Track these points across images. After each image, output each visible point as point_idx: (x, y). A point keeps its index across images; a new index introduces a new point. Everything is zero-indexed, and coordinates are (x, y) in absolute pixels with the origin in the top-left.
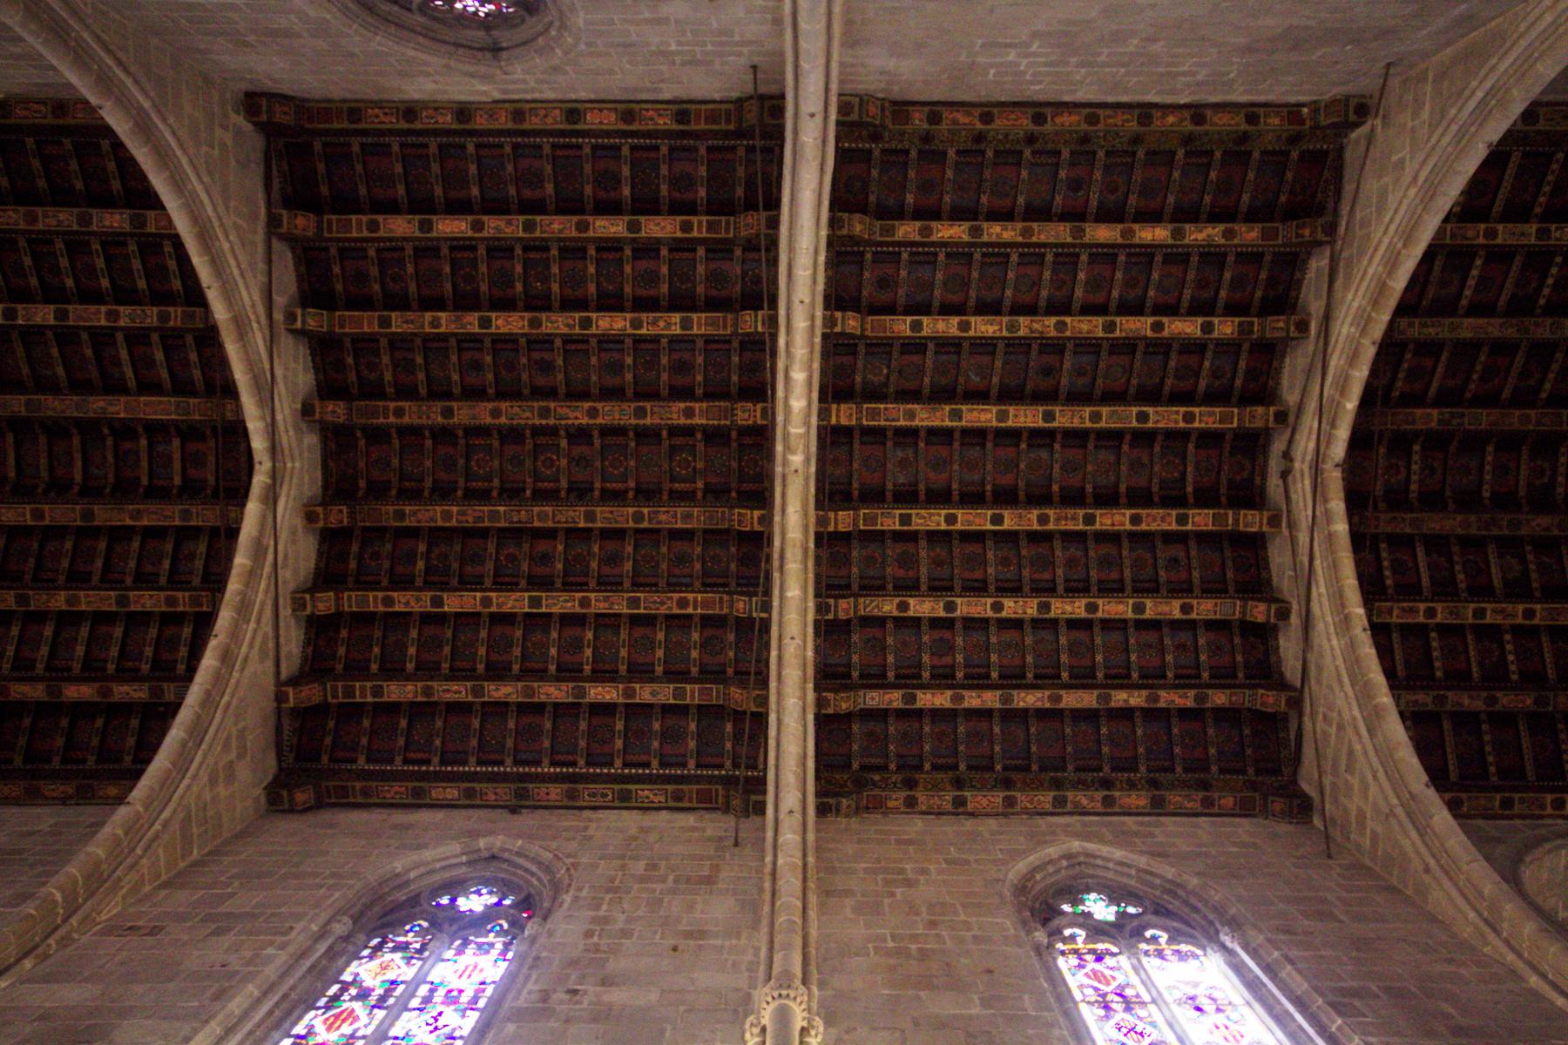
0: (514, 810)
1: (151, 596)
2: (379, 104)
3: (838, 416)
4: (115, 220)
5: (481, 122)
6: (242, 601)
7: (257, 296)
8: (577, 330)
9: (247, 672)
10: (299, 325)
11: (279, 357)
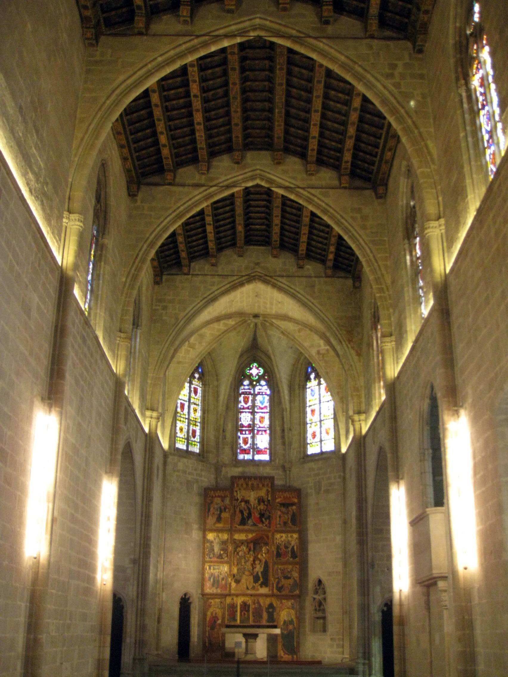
2: (124, 166)
3: (232, 5)
4: (180, 239)
5: (124, 142)
7: (197, 192)
8: (199, 99)
9: (331, 204)
10: (205, 172)
11: (217, 178)
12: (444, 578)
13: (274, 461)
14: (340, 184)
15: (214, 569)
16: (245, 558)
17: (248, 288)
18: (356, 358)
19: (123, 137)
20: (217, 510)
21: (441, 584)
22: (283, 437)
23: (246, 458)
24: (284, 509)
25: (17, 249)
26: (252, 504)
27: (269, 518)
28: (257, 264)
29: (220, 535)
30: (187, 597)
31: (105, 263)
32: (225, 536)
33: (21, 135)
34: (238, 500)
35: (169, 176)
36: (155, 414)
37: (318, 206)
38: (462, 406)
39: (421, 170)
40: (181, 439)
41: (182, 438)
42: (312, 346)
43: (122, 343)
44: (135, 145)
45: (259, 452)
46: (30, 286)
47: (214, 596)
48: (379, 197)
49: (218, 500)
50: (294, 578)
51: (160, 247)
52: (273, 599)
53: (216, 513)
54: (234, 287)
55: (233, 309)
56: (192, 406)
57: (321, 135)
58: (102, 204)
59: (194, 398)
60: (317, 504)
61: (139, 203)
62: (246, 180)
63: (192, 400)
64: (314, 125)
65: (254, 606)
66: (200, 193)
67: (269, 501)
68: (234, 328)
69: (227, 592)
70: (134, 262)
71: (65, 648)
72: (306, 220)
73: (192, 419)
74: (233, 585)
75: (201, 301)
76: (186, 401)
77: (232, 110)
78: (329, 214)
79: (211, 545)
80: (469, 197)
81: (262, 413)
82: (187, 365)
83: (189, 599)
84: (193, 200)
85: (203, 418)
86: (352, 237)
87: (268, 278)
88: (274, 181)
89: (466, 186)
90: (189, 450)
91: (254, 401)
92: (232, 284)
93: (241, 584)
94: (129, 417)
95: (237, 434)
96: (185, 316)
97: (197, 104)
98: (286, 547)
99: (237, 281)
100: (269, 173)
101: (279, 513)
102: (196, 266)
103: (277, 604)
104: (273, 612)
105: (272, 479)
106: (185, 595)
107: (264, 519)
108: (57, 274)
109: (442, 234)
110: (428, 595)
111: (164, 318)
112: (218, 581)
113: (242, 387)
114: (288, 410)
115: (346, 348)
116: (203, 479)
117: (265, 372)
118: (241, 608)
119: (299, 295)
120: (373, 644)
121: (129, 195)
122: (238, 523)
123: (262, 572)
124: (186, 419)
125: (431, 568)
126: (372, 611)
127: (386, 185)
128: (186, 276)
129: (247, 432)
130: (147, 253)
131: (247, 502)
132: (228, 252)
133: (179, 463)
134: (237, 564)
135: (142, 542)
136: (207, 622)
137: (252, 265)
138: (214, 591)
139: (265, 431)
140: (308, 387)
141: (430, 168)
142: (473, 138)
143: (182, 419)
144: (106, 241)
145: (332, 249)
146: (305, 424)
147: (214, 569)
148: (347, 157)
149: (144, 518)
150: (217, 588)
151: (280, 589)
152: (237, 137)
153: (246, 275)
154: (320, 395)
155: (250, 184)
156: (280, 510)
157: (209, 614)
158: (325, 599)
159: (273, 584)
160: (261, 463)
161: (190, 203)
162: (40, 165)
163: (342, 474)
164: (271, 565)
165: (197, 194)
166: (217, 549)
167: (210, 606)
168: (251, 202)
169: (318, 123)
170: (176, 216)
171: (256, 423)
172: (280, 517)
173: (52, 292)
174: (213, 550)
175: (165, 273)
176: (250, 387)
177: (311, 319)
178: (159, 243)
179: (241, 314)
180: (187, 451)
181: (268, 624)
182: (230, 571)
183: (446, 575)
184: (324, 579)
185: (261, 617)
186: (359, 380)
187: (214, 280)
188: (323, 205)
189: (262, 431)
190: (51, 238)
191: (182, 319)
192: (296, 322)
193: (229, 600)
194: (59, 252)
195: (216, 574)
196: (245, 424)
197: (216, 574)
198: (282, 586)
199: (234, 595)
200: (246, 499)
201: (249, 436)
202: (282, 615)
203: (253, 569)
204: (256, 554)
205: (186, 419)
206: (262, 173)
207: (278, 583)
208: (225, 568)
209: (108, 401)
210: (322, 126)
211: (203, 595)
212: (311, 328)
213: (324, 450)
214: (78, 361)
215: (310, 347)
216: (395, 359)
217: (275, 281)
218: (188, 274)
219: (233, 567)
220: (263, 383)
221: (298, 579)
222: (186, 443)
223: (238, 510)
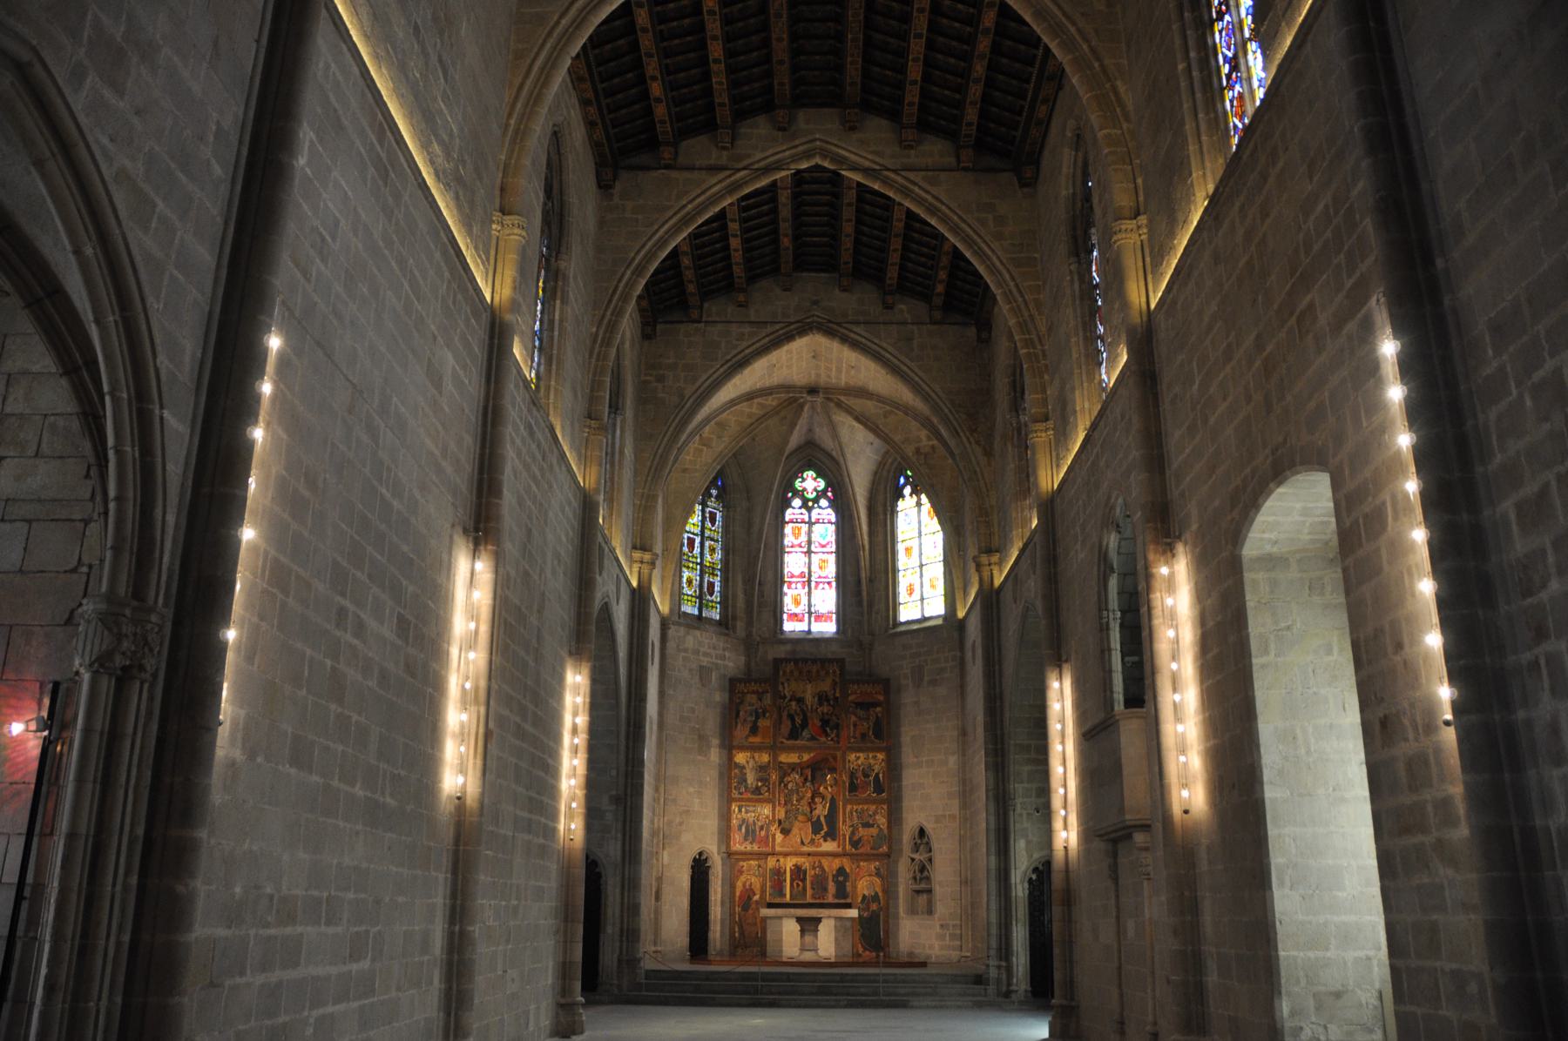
0: (1060, 87)
2: (590, 137)
5: (590, 95)
6: (902, 192)
7: (714, 180)
8: (718, 17)
11: (749, 156)
12: (1146, 827)
14: (959, 161)
15: (747, 812)
16: (798, 793)
17: (801, 345)
19: (588, 85)
20: (751, 715)
21: (1139, 838)
22: (859, 593)
24: (861, 713)
25: (417, 273)
26: (809, 704)
27: (837, 726)
28: (815, 303)
29: (756, 755)
30: (704, 857)
31: (562, 302)
32: (765, 758)
33: (418, 75)
34: (785, 697)
35: (666, 153)
36: (647, 557)
37: (920, 201)
38: (1179, 537)
39: (1105, 131)
41: (692, 596)
43: (592, 437)
44: (609, 100)
45: (819, 618)
46: (439, 338)
48: (1023, 185)
50: (878, 826)
51: (652, 276)
52: (845, 860)
53: (749, 719)
54: (776, 343)
55: (776, 379)
56: (707, 544)
57: (926, 78)
58: (555, 202)
61: (616, 200)
62: (797, 158)
63: (707, 533)
64: (915, 60)
65: (813, 872)
66: (720, 181)
67: (836, 699)
68: (775, 411)
69: (769, 850)
70: (610, 301)
71: (510, 946)
72: (898, 225)
74: (779, 837)
76: (696, 535)
77: (774, 36)
79: (741, 772)
80: (1194, 175)
84: (708, 194)
85: (725, 561)
86: (980, 254)
87: (835, 327)
88: (845, 158)
89: (1188, 156)
91: (809, 533)
92: (772, 337)
93: (791, 835)
94: (606, 562)
96: (693, 394)
97: (714, 26)
98: (866, 776)
99: (781, 332)
100: (836, 145)
101: (853, 718)
104: (846, 880)
105: (841, 662)
106: (700, 854)
108: (485, 317)
109: (1142, 241)
110: (1115, 855)
111: (660, 395)
112: (754, 831)
113: (789, 511)
114: (867, 547)
115: (968, 445)
116: (726, 662)
119: (887, 355)
120: (1015, 934)
121: (600, 186)
122: (786, 735)
123: (825, 817)
124: (697, 564)
125: (1122, 810)
126: (1013, 881)
127: (1037, 163)
128: (696, 325)
129: (799, 586)
130: (631, 285)
131: (800, 701)
134: (785, 804)
136: (737, 899)
138: (749, 847)
139: (829, 583)
140: (899, 509)
141: (1121, 128)
142: (1201, 71)
143: (691, 565)
144: (563, 265)
145: (943, 275)
146: (895, 571)
147: (747, 812)
148: (971, 114)
149: (631, 729)
150: (751, 843)
151: (855, 844)
152: (781, 84)
153: (798, 322)
154: (920, 522)
155: (804, 166)
156: (856, 715)
157: (739, 884)
158: (930, 860)
159: (844, 835)
162: (452, 130)
163: (958, 654)
165: (716, 184)
166: (751, 778)
167: (741, 872)
169: (922, 57)
170: (680, 221)
171: (813, 569)
172: (855, 725)
173: (476, 349)
174: (745, 781)
175: (660, 320)
176: (803, 511)
177: (906, 395)
178: (652, 269)
179: (786, 388)
180: (700, 617)
181: (836, 901)
183: (1149, 822)
184: (929, 827)
185: (825, 890)
186: (988, 496)
188: (929, 198)
189: (824, 583)
190: (472, 256)
191: (690, 397)
192: (880, 399)
193: (771, 862)
194: (487, 281)
195: (751, 820)
196: (797, 574)
197: (751, 820)
199: (780, 854)
200: (799, 695)
203: (811, 812)
204: (816, 785)
205: (697, 564)
206: (825, 145)
207: (853, 833)
208: (766, 810)
209: (571, 533)
210: (928, 63)
211: (729, 854)
212: (907, 410)
213: (927, 615)
214: (521, 467)
215: (903, 443)
216: (1054, 460)
218: (699, 322)
220: (824, 503)
221: (884, 827)
223: (785, 714)
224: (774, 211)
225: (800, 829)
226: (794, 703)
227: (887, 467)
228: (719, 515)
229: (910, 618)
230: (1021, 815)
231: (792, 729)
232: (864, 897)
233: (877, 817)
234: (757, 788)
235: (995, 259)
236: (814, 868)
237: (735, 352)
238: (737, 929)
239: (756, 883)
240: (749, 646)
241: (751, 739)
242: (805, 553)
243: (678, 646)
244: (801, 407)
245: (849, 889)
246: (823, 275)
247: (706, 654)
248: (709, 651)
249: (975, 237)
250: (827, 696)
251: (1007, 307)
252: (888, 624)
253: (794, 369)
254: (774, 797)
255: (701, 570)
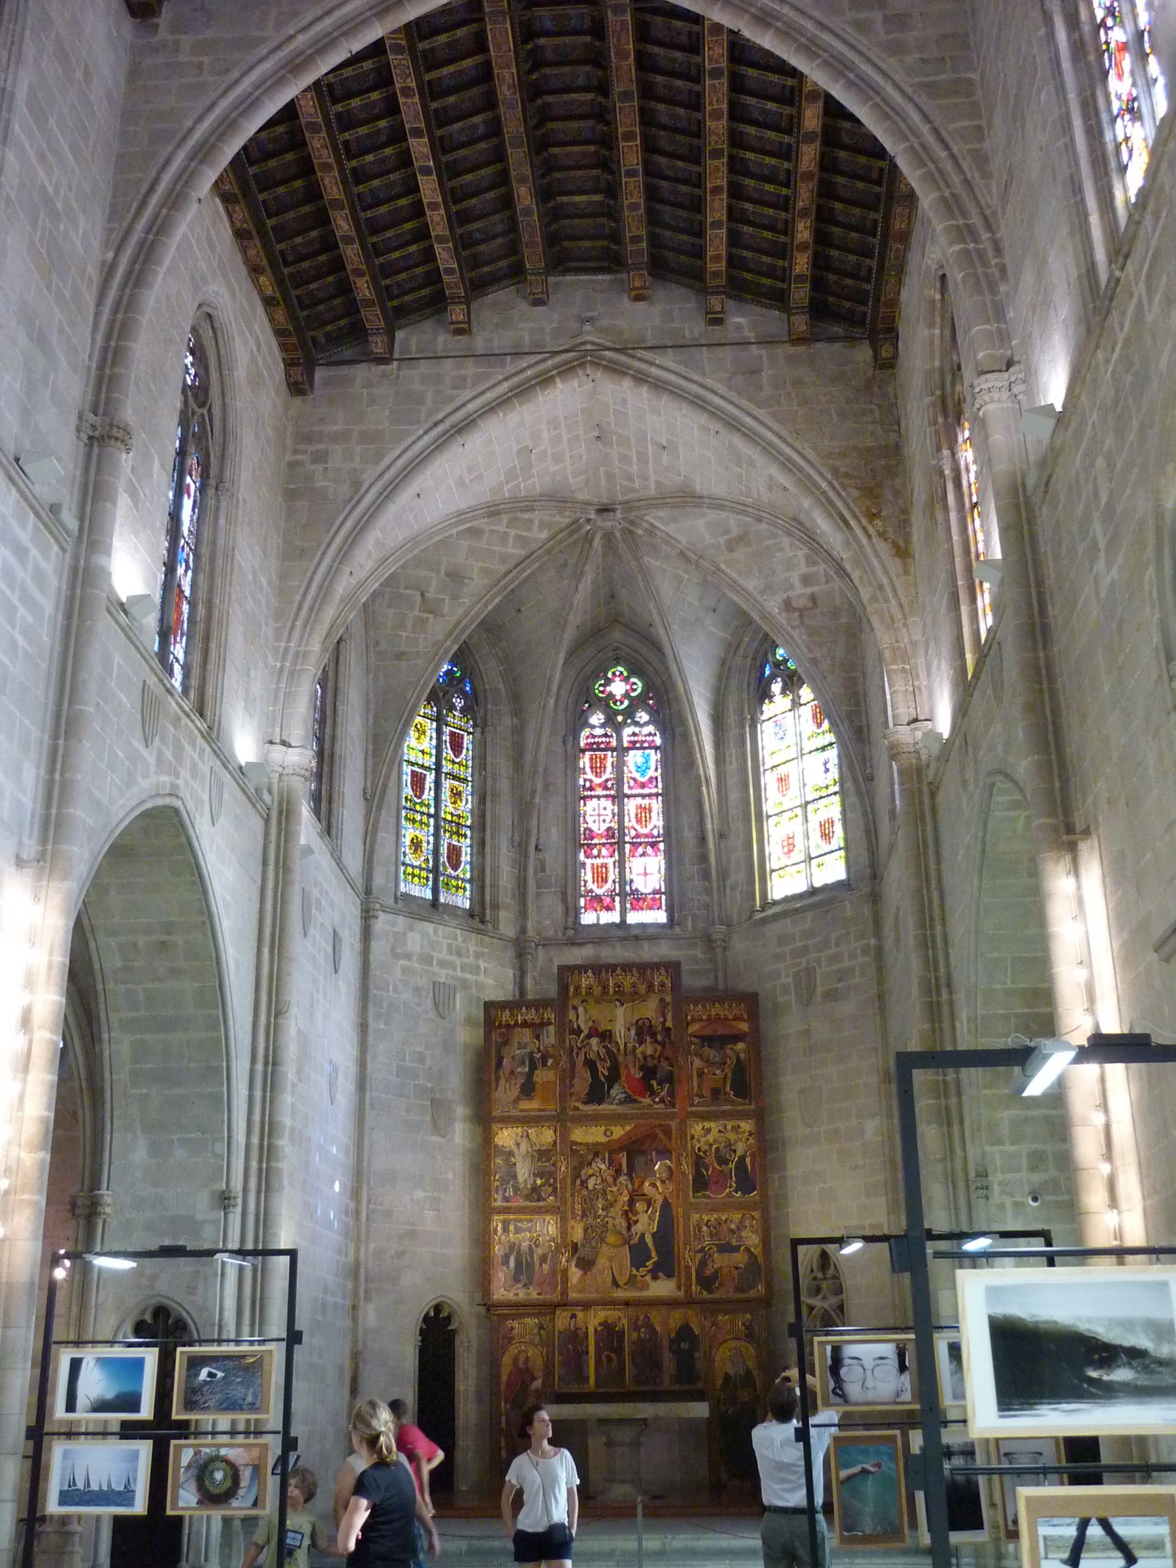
1: (709, 49)
13: (679, 924)
15: (517, 1231)
18: (894, 565)
20: (523, 1063)
22: (703, 858)
23: (602, 922)
26: (621, 1043)
27: (670, 1078)
28: (590, 320)
29: (532, 1132)
30: (444, 1314)
32: (547, 1136)
34: (579, 1031)
40: (417, 871)
41: (421, 869)
42: (768, 588)
45: (638, 900)
47: (520, 1309)
49: (526, 1035)
50: (748, 1250)
52: (690, 1312)
53: (519, 1070)
54: (522, 392)
56: (447, 784)
59: (454, 762)
60: (806, 1033)
61: (163, 33)
63: (447, 767)
65: (635, 1335)
67: (668, 1029)
69: (555, 1297)
70: (143, 204)
73: (449, 817)
74: (575, 1274)
75: (425, 433)
76: (429, 769)
78: (779, 24)
79: (507, 1161)
81: (643, 796)
82: (420, 661)
83: (448, 1319)
87: (622, 358)
90: (442, 900)
91: (619, 767)
92: (516, 380)
95: (575, 856)
96: (377, 479)
99: (529, 373)
101: (698, 1063)
102: (408, 338)
103: (703, 1329)
105: (672, 968)
106: (438, 1308)
107: (654, 1083)
112: (530, 1265)
113: (586, 732)
114: (713, 780)
115: (864, 540)
116: (482, 978)
117: (647, 688)
118: (596, 1343)
119: (716, 400)
123: (654, 1235)
124: (429, 816)
128: (383, 367)
130: (186, 179)
131: (606, 1036)
132: (502, 295)
133: (410, 934)
134: (584, 1215)
135: (255, 1140)
136: (503, 1387)
137: (574, 325)
138: (520, 1294)
139: (653, 845)
143: (418, 817)
145: (803, 231)
147: (517, 1231)
149: (260, 1067)
150: (525, 1286)
151: (707, 1282)
157: (507, 1361)
160: (644, 934)
161: (327, 23)
163: (873, 942)
164: (679, 1211)
166: (523, 1172)
168: (549, 99)
172: (700, 1075)
174: (515, 1177)
176: (609, 731)
179: (558, 499)
181: (677, 1387)
182: (564, 1232)
185: (658, 1367)
186: (906, 625)
187: (463, 372)
193: (562, 1320)
195: (525, 1245)
196: (599, 828)
197: (525, 1245)
198: (715, 1275)
199: (577, 1304)
200: (602, 1027)
201: (610, 861)
202: (718, 1359)
203: (629, 1228)
205: (429, 816)
207: (703, 1264)
208: (548, 1228)
211: (489, 1306)
217: (644, 366)
219: (572, 1223)
220: (643, 716)
222: (430, 883)
224: (495, 129)
225: (611, 1259)
226: (594, 1041)
227: (741, 652)
228: (467, 740)
229: (790, 893)
230: (1002, 1206)
231: (591, 1085)
232: (727, 1377)
233: (744, 1234)
234: (535, 1189)
235: (889, 89)
236: (637, 1329)
237: (448, 409)
238: (503, 1444)
239: (535, 1355)
240: (521, 950)
241: (525, 1105)
242: (613, 798)
243: (393, 948)
244: (588, 539)
245: (699, 1365)
246: (600, 277)
247: (442, 964)
248: (449, 958)
249: (849, 54)
250: (651, 1026)
251: (919, 172)
252: (754, 905)
253: (568, 462)
254: (564, 1201)
255: (437, 828)
